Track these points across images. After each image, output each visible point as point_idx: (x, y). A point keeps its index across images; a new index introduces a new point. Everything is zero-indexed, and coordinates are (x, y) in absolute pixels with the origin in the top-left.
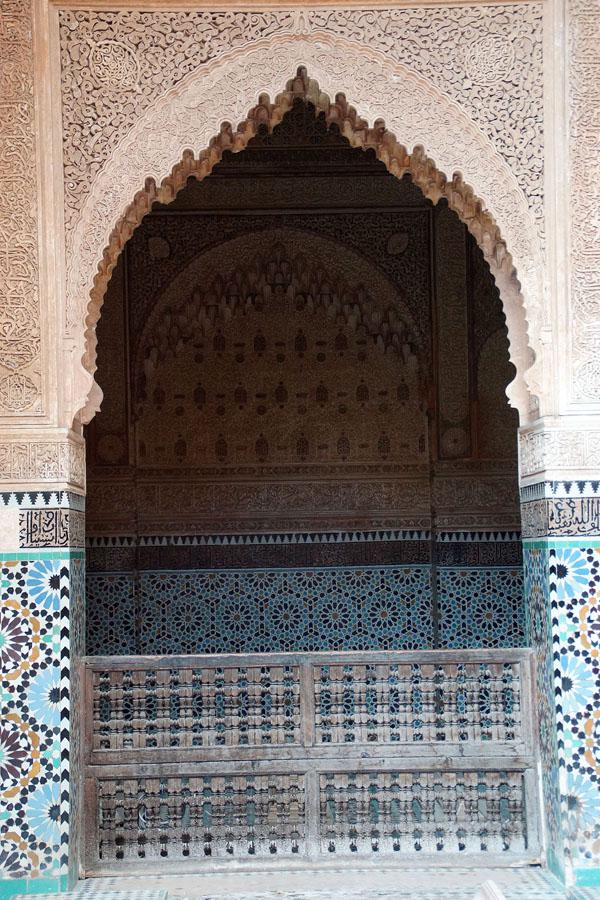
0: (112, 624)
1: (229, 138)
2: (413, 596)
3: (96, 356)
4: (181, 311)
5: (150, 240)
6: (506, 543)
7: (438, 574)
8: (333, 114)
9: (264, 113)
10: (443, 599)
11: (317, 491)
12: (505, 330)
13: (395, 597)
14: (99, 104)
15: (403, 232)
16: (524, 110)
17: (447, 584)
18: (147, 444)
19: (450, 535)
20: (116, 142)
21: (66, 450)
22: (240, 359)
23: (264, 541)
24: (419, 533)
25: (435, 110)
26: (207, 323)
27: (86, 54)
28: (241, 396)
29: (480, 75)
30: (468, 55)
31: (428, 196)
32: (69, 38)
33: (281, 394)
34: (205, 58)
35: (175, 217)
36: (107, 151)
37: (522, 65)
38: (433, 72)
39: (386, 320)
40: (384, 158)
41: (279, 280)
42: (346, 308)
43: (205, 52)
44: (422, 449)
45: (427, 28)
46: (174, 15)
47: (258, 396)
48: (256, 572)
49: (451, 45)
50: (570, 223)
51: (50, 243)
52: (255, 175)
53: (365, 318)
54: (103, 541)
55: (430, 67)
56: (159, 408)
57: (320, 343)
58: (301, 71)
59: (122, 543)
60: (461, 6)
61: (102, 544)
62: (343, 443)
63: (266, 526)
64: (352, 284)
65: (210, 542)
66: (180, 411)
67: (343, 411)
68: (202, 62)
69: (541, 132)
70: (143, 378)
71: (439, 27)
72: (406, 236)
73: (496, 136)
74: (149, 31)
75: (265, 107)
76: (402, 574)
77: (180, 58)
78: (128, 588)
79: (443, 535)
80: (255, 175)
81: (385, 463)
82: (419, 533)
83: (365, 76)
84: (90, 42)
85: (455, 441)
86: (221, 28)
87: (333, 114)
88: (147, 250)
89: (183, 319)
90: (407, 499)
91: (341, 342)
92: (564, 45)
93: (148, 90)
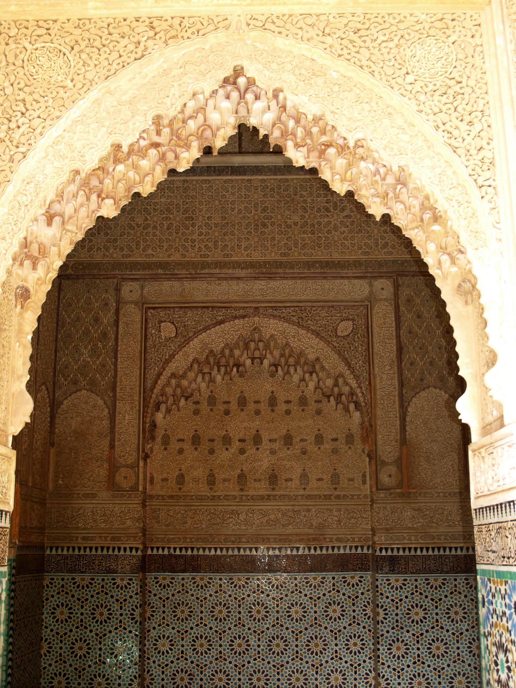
0: (121, 615)
1: (173, 155)
2: (357, 597)
3: (29, 365)
4: (184, 376)
5: (162, 324)
6: (430, 556)
7: (377, 580)
8: (276, 133)
9: (208, 133)
10: (381, 601)
11: (283, 515)
13: (343, 598)
14: (29, 99)
15: (349, 320)
16: (470, 104)
17: (384, 588)
18: (155, 476)
19: (387, 549)
20: (41, 134)
22: (227, 413)
23: (242, 552)
24: (362, 547)
25: (377, 103)
26: (203, 385)
27: (21, 56)
28: (227, 440)
29: (422, 71)
30: (409, 53)
31: (370, 211)
32: (7, 44)
33: (257, 440)
35: (181, 308)
36: (32, 142)
37: (464, 65)
38: (374, 68)
39: (336, 384)
40: (326, 175)
41: (257, 354)
42: (307, 376)
43: (140, 50)
44: (364, 482)
45: (367, 29)
46: (112, 21)
47: (240, 441)
48: (236, 576)
49: (391, 45)
52: (239, 278)
53: (321, 383)
54: (116, 550)
55: (370, 63)
56: (165, 449)
57: (287, 402)
59: (131, 552)
60: (399, 12)
61: (116, 552)
62: (304, 476)
63: (244, 540)
64: (311, 357)
65: (201, 552)
66: (181, 451)
67: (304, 453)
68: (136, 59)
70: (154, 425)
71: (378, 29)
72: (351, 322)
73: (443, 128)
74: (86, 35)
75: (209, 126)
76: (349, 580)
77: (115, 55)
78: (135, 586)
79: (381, 550)
80: (239, 278)
81: (337, 493)
82: (362, 547)
83: (304, 72)
84: (27, 45)
85: (390, 476)
86: (157, 30)
87: (276, 133)
88: (160, 331)
89: (185, 383)
90: (353, 521)
91: (303, 401)
93: (80, 85)
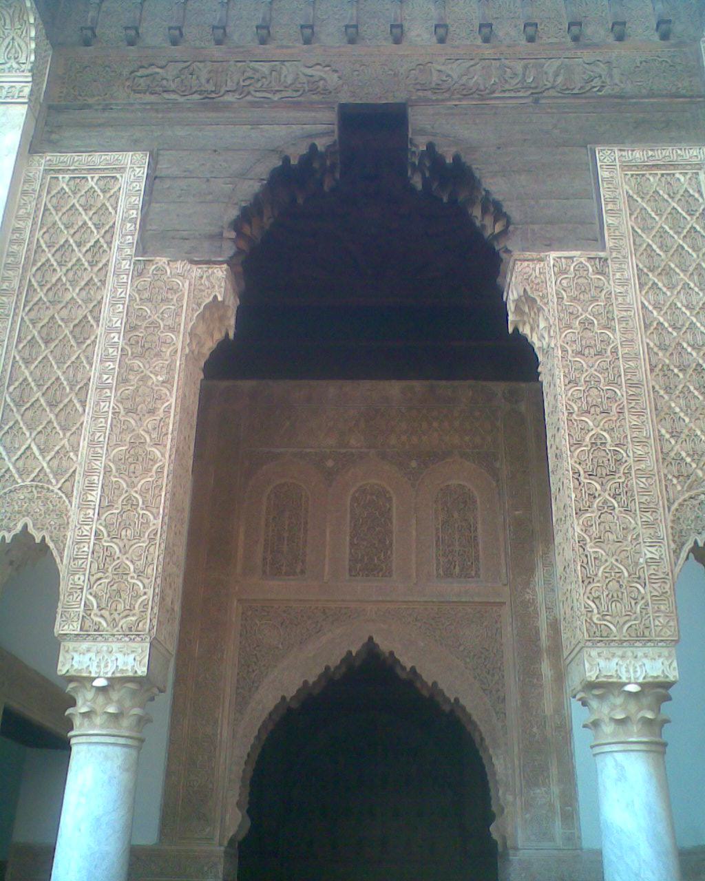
3: (248, 798)
12: (489, 790)
21: (222, 860)
34: (318, 630)
50: (520, 731)
51: (225, 732)
58: (371, 639)
69: (503, 677)
84: (258, 622)
92: (512, 629)
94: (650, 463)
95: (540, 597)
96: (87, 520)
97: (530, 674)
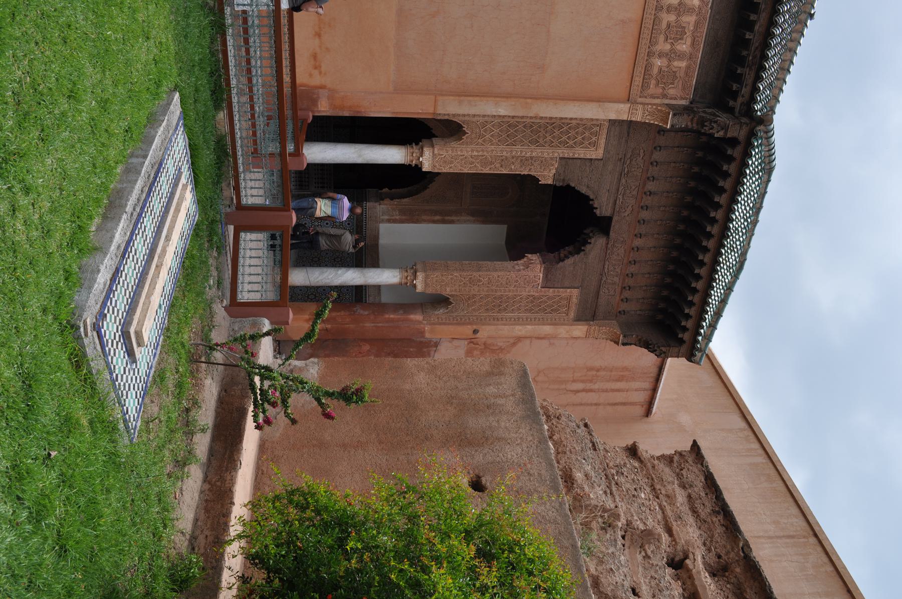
94: (472, 292)
95: (462, 218)
96: (468, 152)
97: (436, 213)
